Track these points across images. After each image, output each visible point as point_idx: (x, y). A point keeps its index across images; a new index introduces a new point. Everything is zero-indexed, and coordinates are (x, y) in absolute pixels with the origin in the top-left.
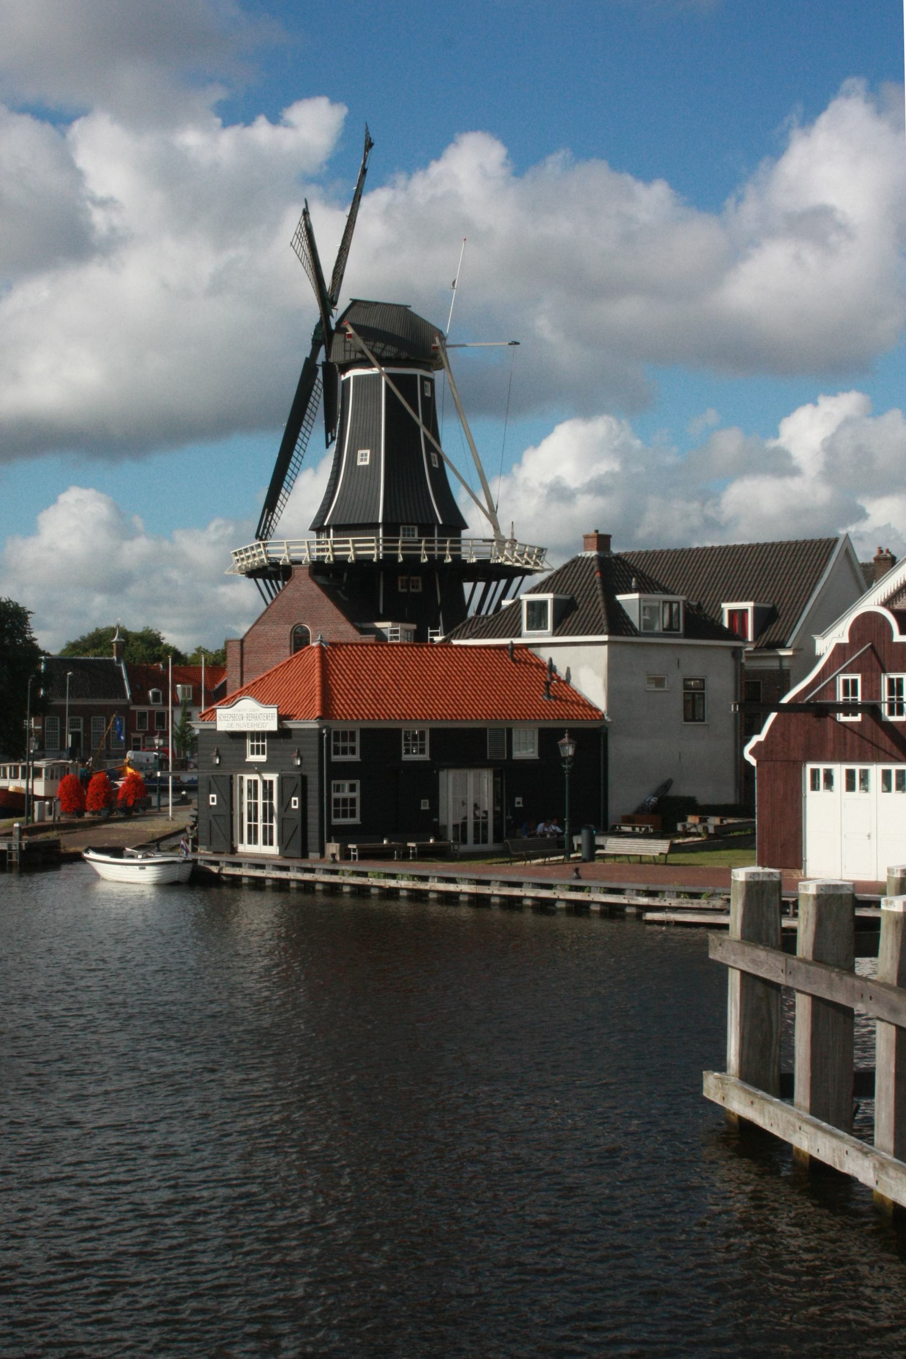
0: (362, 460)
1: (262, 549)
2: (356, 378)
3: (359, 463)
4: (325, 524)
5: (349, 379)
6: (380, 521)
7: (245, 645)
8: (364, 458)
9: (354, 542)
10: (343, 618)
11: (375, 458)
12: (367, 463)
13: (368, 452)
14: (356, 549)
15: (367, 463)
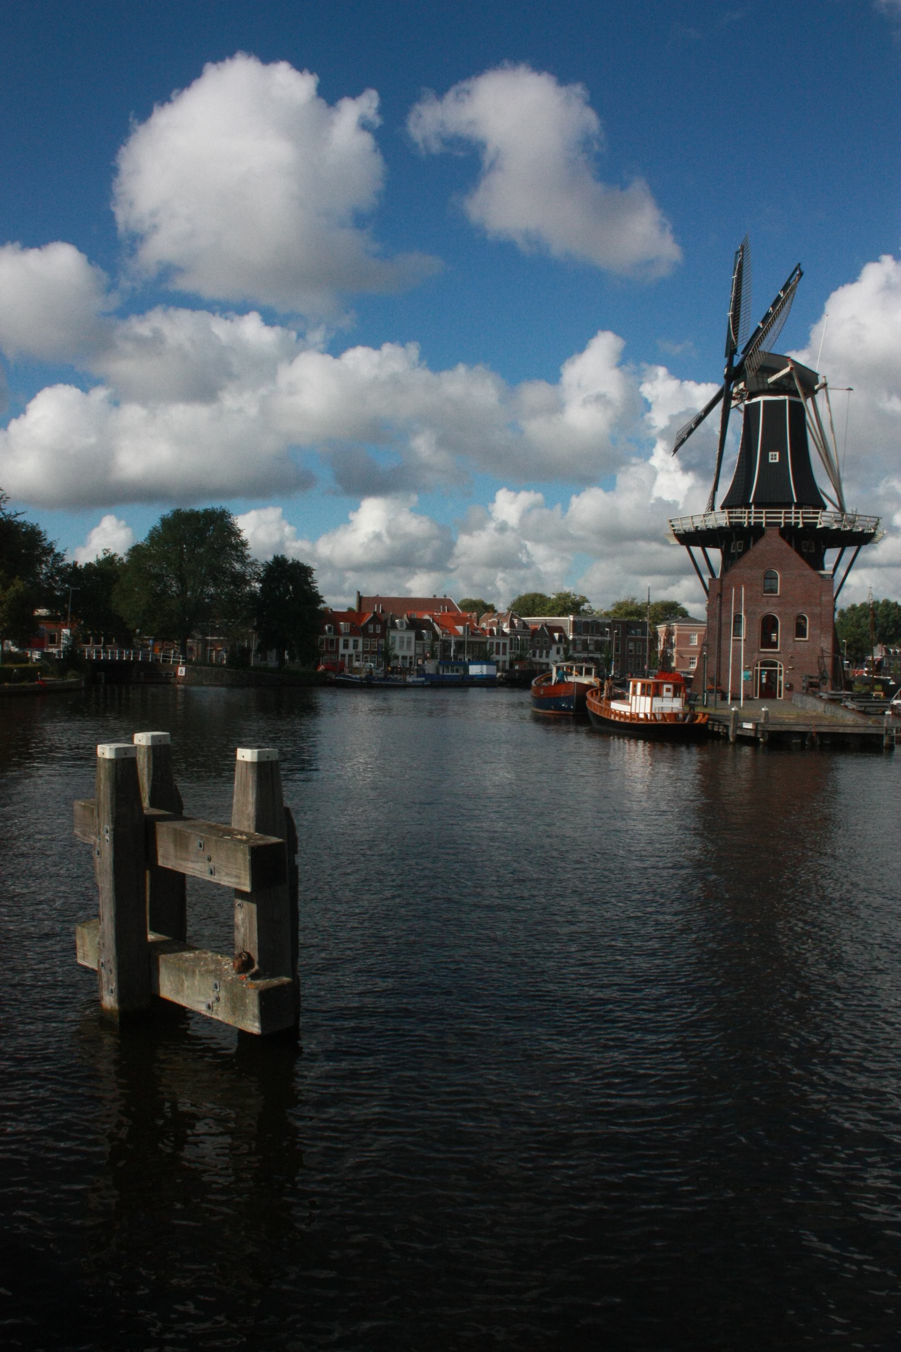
0: (772, 459)
1: (746, 515)
2: (765, 402)
3: (771, 461)
4: (751, 501)
5: (759, 403)
6: (795, 501)
7: (724, 583)
8: (774, 457)
9: (803, 513)
10: (807, 566)
11: (783, 457)
12: (777, 461)
13: (777, 454)
14: (804, 518)
15: (777, 461)
